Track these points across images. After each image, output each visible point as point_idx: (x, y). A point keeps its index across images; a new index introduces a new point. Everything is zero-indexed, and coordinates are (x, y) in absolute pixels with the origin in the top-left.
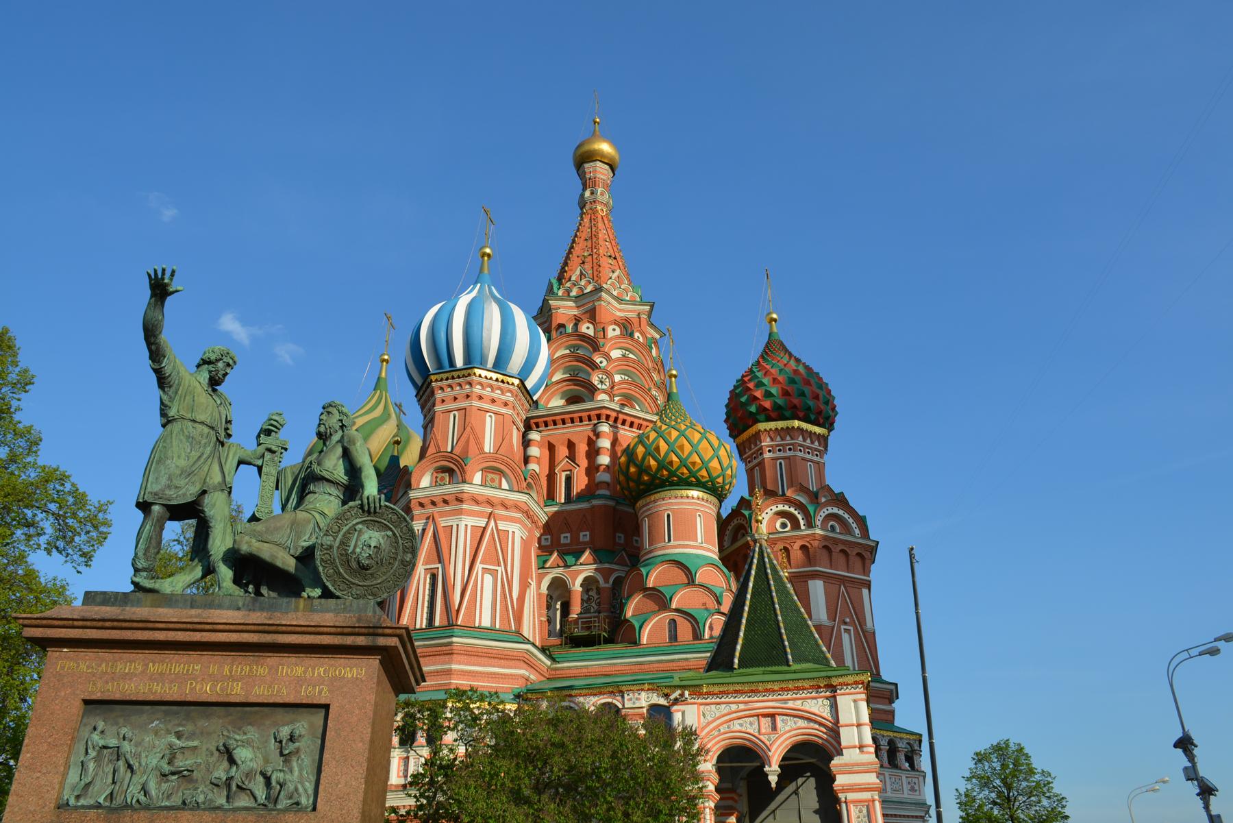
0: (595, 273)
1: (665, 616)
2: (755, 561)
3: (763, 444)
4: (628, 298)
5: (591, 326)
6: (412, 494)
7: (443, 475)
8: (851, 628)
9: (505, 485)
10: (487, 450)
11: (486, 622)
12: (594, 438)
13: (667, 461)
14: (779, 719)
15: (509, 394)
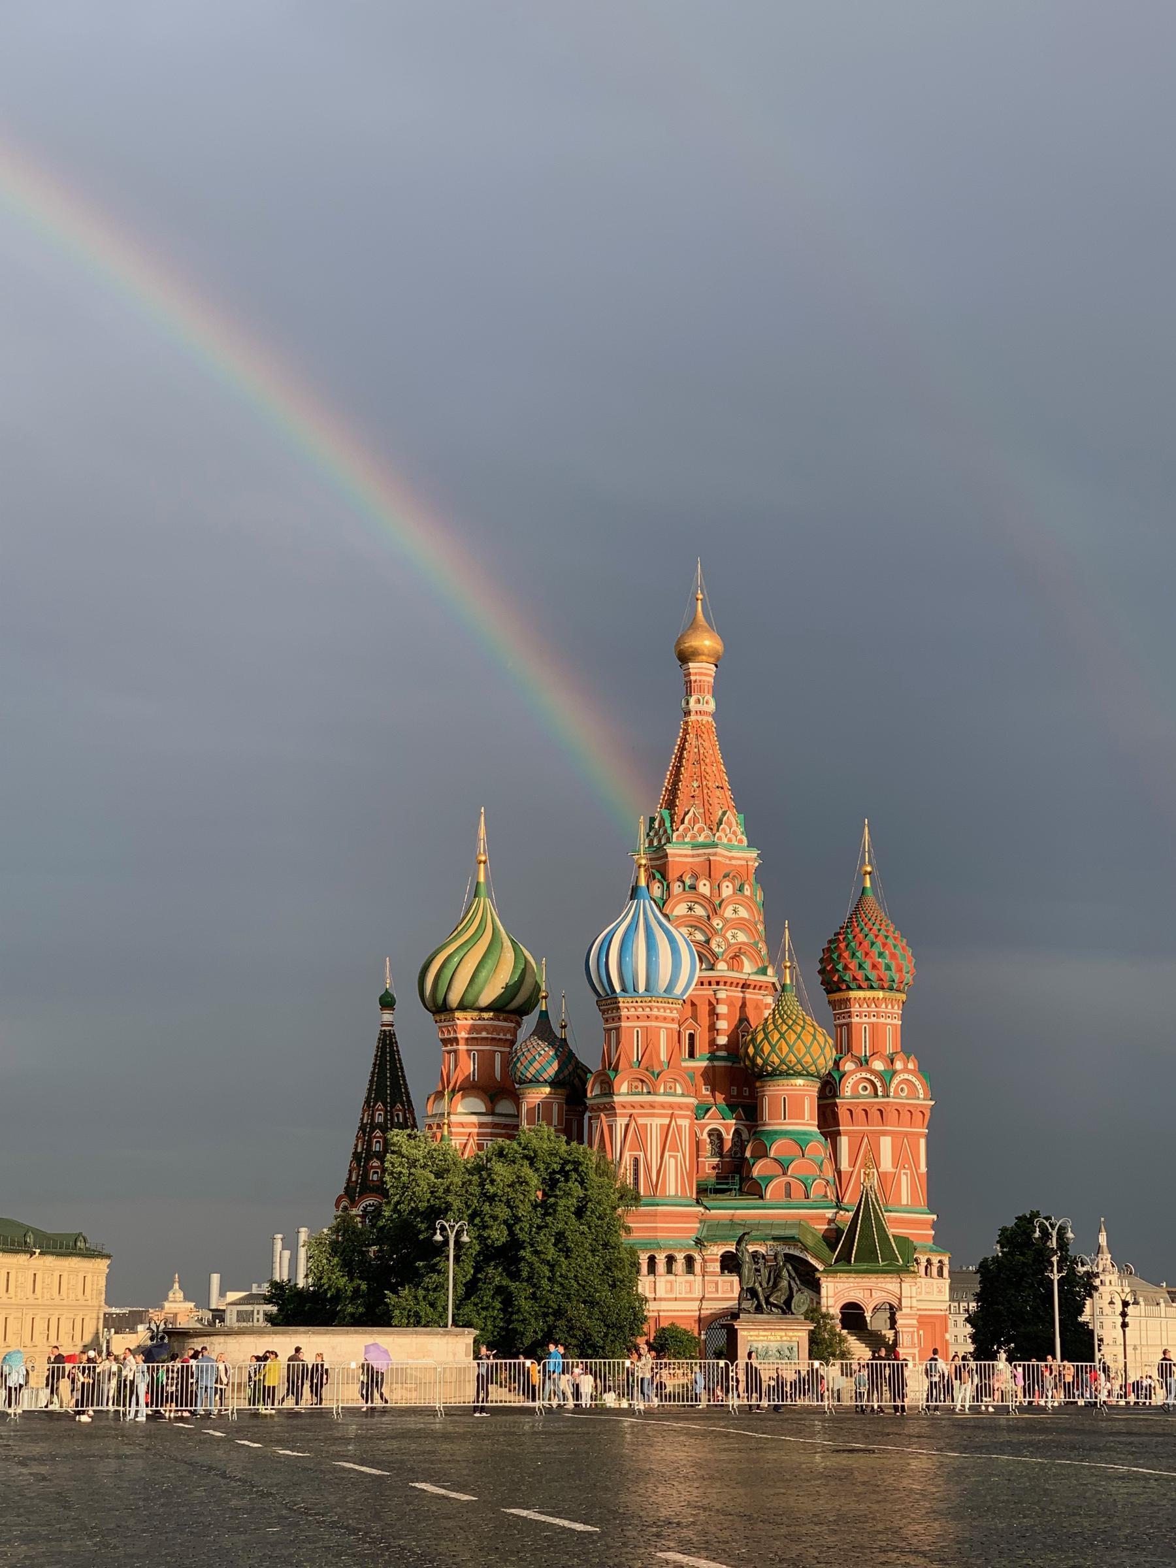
0: (707, 815)
1: (785, 1179)
2: (863, 1199)
3: (852, 1009)
4: (736, 843)
5: (707, 883)
6: (616, 1099)
7: (636, 1084)
8: (909, 1172)
9: (679, 1091)
10: (662, 1059)
11: (673, 1193)
12: (714, 1002)
13: (787, 1059)
14: (873, 1291)
15: (675, 1012)
